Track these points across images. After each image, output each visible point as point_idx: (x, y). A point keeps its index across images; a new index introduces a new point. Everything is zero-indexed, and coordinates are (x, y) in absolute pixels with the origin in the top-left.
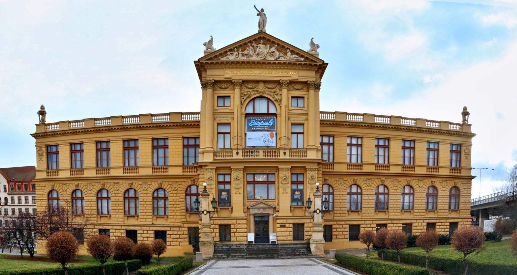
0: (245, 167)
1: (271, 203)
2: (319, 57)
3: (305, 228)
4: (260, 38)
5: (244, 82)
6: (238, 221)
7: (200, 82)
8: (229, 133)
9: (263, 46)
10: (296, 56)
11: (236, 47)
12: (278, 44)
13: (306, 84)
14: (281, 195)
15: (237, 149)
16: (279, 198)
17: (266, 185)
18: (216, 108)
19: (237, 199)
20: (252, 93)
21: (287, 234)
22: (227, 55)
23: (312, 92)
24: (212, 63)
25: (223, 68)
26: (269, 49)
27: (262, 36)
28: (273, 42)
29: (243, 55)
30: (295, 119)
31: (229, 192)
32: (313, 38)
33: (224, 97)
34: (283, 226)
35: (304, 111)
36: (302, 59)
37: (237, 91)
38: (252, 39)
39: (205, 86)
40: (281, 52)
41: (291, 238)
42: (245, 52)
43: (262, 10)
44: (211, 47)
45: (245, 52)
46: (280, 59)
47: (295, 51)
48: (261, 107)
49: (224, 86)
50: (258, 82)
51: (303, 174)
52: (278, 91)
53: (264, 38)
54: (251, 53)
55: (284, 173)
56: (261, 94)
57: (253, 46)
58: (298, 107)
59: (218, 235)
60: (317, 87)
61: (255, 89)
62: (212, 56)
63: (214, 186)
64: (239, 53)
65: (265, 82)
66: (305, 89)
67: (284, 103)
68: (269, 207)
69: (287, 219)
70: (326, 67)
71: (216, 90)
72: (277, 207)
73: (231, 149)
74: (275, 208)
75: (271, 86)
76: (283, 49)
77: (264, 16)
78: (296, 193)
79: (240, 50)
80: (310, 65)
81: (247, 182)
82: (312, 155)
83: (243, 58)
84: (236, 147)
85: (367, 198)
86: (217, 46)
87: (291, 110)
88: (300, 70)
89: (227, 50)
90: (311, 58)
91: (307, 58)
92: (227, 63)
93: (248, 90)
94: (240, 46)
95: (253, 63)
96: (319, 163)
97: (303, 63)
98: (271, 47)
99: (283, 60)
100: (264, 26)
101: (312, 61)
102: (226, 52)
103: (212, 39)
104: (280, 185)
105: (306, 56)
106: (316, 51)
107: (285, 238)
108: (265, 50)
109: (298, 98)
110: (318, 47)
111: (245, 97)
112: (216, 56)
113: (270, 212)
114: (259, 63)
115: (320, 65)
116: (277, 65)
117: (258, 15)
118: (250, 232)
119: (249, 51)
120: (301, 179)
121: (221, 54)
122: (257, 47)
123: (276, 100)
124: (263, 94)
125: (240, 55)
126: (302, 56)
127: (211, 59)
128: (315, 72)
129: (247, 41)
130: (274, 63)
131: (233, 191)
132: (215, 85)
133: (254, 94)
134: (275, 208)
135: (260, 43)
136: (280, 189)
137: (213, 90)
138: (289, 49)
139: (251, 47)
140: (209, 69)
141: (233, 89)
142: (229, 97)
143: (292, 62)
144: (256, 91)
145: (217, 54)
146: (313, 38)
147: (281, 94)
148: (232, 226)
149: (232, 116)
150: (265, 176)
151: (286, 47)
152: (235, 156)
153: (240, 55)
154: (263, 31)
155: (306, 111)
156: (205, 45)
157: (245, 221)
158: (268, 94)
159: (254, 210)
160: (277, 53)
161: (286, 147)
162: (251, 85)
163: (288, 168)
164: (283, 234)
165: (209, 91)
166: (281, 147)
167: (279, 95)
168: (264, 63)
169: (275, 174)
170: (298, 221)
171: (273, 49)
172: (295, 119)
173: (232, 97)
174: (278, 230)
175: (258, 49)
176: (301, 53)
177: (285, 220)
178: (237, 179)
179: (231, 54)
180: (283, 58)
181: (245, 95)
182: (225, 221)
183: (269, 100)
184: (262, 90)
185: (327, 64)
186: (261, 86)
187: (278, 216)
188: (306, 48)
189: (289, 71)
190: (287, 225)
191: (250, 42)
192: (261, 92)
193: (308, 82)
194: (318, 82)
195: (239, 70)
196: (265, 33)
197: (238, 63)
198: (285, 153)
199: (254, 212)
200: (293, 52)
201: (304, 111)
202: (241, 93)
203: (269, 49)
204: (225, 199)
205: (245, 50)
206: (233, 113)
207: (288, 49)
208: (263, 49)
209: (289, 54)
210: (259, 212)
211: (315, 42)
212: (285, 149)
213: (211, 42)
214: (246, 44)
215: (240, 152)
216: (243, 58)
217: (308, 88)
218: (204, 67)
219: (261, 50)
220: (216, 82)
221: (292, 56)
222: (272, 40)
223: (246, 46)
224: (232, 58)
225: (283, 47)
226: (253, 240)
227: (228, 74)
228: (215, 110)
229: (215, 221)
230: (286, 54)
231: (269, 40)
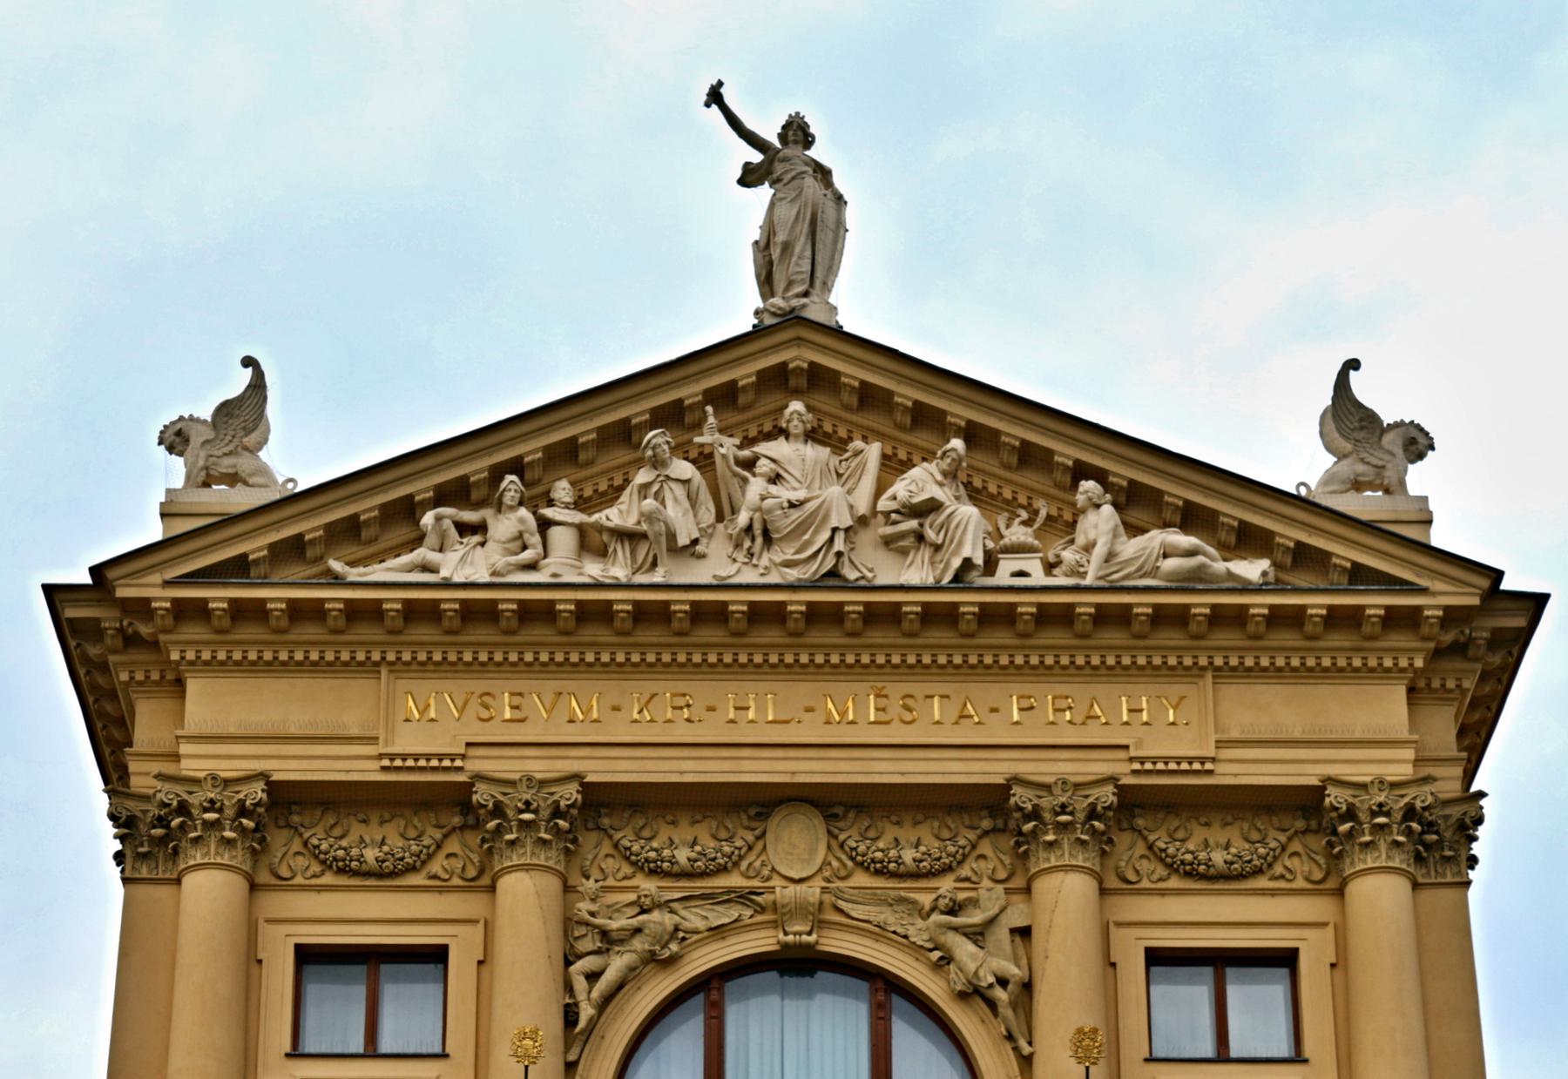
2: (1440, 537)
4: (778, 380)
5: (602, 804)
7: (103, 802)
9: (816, 453)
11: (516, 466)
12: (973, 435)
20: (694, 918)
22: (418, 540)
23: (1381, 893)
25: (370, 668)
26: (878, 493)
27: (798, 357)
29: (591, 543)
32: (1353, 364)
33: (371, 961)
36: (1252, 569)
37: (525, 895)
38: (690, 392)
39: (151, 839)
40: (1011, 506)
42: (616, 516)
44: (243, 463)
45: (616, 516)
46: (1003, 574)
47: (1158, 484)
49: (373, 841)
50: (760, 804)
52: (991, 898)
56: (798, 932)
57: (704, 460)
60: (1440, 839)
61: (734, 880)
62: (255, 547)
64: (544, 525)
66: (1302, 868)
67: (1064, 1006)
70: (1523, 638)
71: (283, 884)
75: (911, 843)
76: (1030, 478)
79: (563, 490)
83: (593, 569)
88: (1224, 673)
89: (421, 487)
90: (1344, 554)
91: (1304, 556)
93: (649, 885)
97: (1260, 603)
98: (893, 466)
99: (1038, 577)
100: (820, 274)
101: (1359, 576)
102: (408, 510)
103: (258, 386)
105: (1288, 534)
106: (1395, 488)
108: (835, 490)
109: (1221, 963)
110: (1417, 443)
111: (617, 965)
112: (295, 549)
114: (762, 615)
115: (1452, 616)
116: (971, 631)
117: (750, 177)
119: (664, 495)
121: (349, 531)
122: (749, 464)
123: (973, 994)
124: (820, 925)
125: (562, 539)
126: (1248, 540)
127: (238, 568)
128: (1398, 693)
129: (637, 410)
130: (938, 616)
132: (278, 839)
133: (718, 932)
135: (781, 432)
137: (254, 887)
138: (1100, 476)
139: (683, 469)
140: (212, 666)
141: (484, 883)
142: (436, 956)
143: (1142, 604)
144: (744, 897)
145: (310, 526)
146: (1353, 364)
147: (1024, 933)
151: (1067, 453)
153: (562, 539)
154: (814, 313)
156: (175, 439)
158: (880, 933)
160: (968, 512)
162: (683, 843)
165: (207, 889)
167: (1001, 934)
171: (921, 482)
173: (460, 964)
175: (756, 486)
176: (1232, 513)
179: (464, 529)
180: (1034, 566)
181: (609, 941)
183: (886, 990)
184: (812, 892)
185: (1537, 603)
186: (796, 855)
188: (1295, 459)
189: (1101, 690)
192: (800, 910)
193: (1336, 797)
194: (1449, 787)
195: (550, 686)
196: (838, 332)
197: (533, 614)
200: (1138, 507)
202: (569, 923)
203: (878, 493)
205: (611, 496)
207: (1081, 471)
208: (799, 472)
209: (1100, 523)
213: (244, 413)
214: (624, 435)
216: (593, 569)
217: (1335, 859)
219: (784, 493)
220: (288, 802)
221: (1131, 547)
222: (906, 394)
223: (622, 456)
224: (466, 565)
225: (1031, 452)
227: (427, 722)
230: (1064, 525)
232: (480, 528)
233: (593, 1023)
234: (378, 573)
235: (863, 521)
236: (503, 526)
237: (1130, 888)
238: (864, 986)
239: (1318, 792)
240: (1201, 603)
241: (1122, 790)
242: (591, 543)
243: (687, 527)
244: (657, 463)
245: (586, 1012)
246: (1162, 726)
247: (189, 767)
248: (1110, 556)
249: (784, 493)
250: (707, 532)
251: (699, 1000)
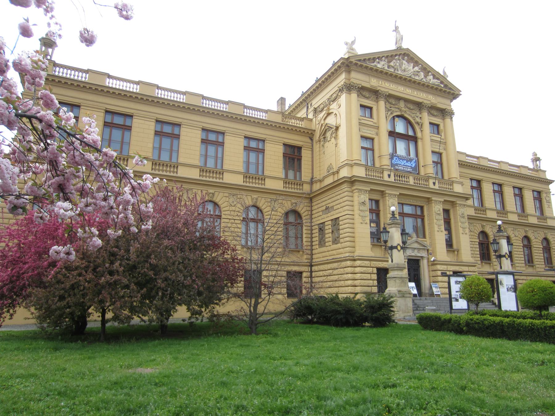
52: (418, 114)
55: (438, 206)
65: (406, 101)
80: (449, 93)
88: (438, 96)
113: (424, 254)
123: (418, 123)
140: (355, 71)
149: (376, 130)
206: (378, 128)
210: (413, 254)
227: (374, 82)
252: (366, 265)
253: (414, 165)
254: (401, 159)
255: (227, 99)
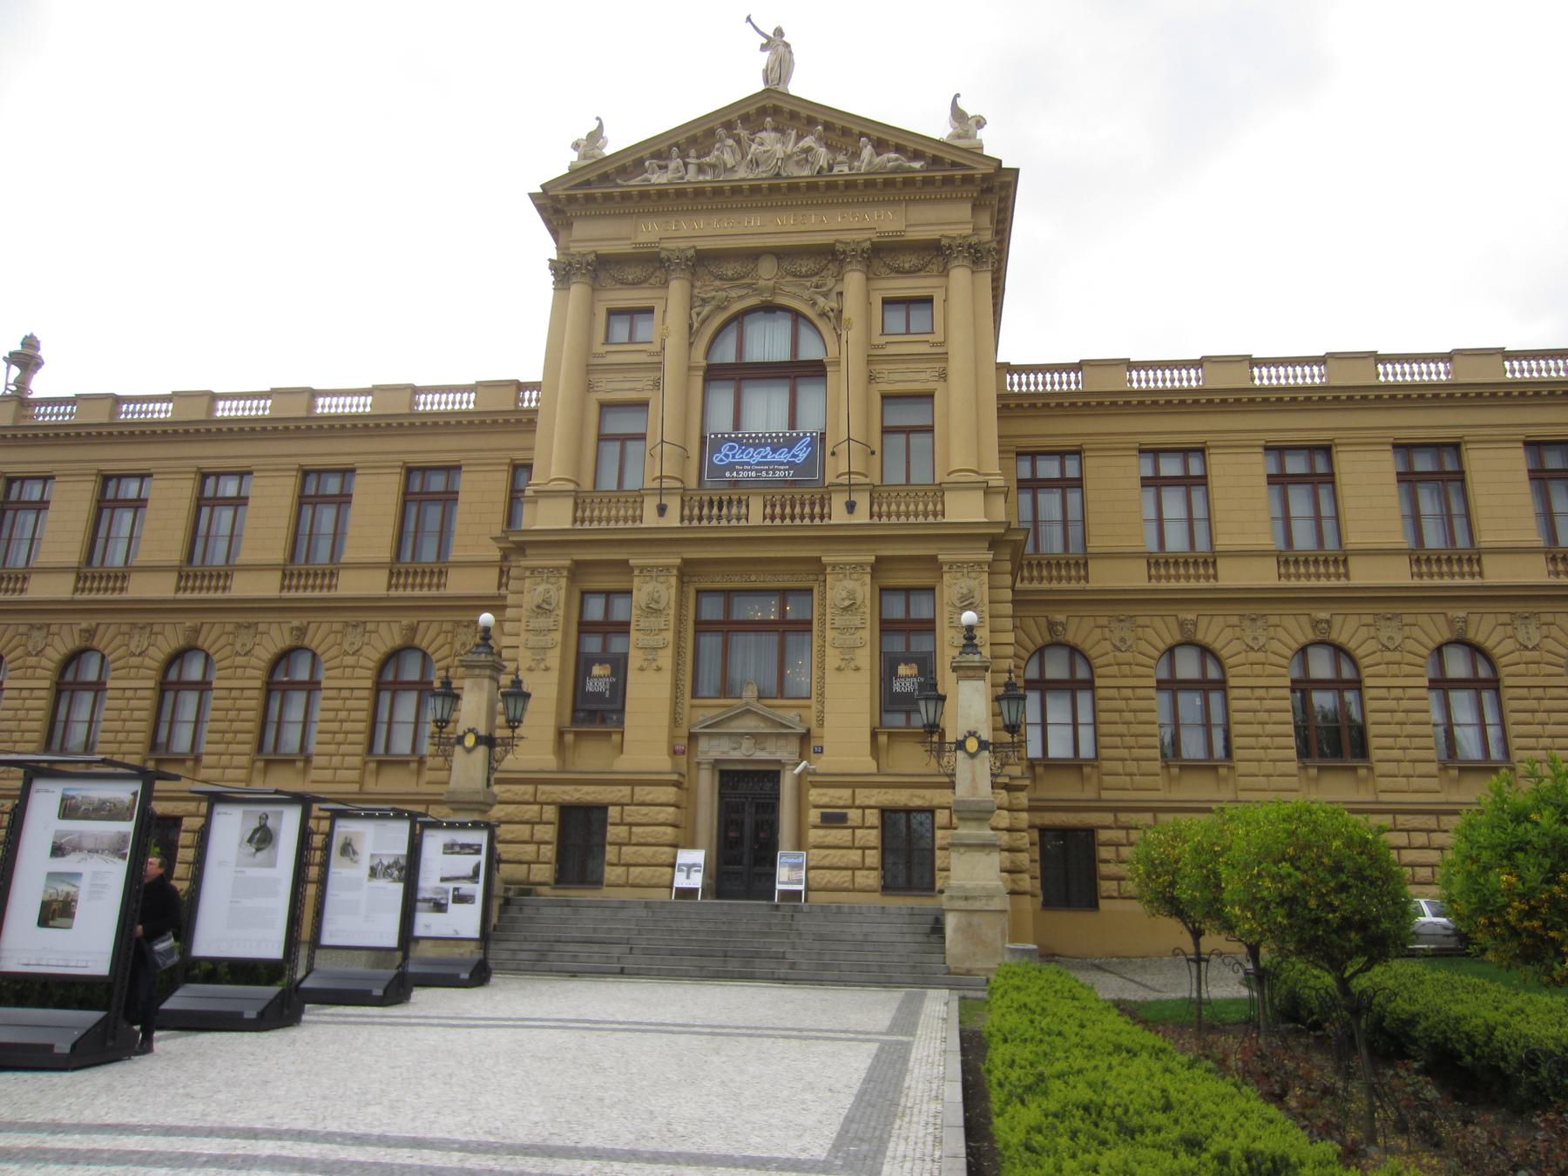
0: (686, 562)
1: (791, 715)
3: (939, 833)
4: (763, 112)
6: (642, 793)
8: (641, 437)
10: (893, 155)
11: (677, 145)
13: (936, 253)
14: (830, 676)
15: (661, 491)
16: (822, 694)
17: (773, 639)
18: (599, 348)
19: (649, 693)
20: (733, 294)
21: (854, 856)
24: (589, 199)
27: (769, 103)
28: (811, 122)
30: (897, 377)
31: (619, 666)
34: (833, 819)
35: (934, 345)
37: (677, 290)
38: (733, 116)
41: (872, 879)
43: (779, 32)
46: (835, 171)
48: (768, 342)
49: (631, 274)
50: (753, 255)
51: (932, 589)
52: (830, 282)
53: (776, 111)
54: (728, 159)
56: (767, 297)
57: (738, 141)
58: (908, 332)
59: (549, 852)
63: (558, 636)
64: (686, 165)
65: (782, 254)
68: (781, 732)
69: (853, 786)
72: (815, 731)
73: (639, 496)
74: (805, 738)
75: (805, 266)
77: (781, 49)
78: (903, 670)
79: (693, 152)
81: (697, 622)
82: (965, 509)
84: (656, 484)
85: (1255, 704)
86: (615, 143)
87: (882, 347)
92: (644, 195)
93: (717, 283)
94: (693, 141)
95: (736, 190)
96: (994, 542)
98: (800, 137)
99: (846, 170)
104: (830, 634)
107: (841, 877)
108: (778, 146)
113: (783, 752)
114: (755, 190)
116: (825, 191)
118: (692, 845)
120: (921, 609)
121: (623, 171)
123: (823, 315)
125: (692, 169)
127: (588, 183)
130: (812, 187)
131: (633, 663)
133: (741, 298)
134: (805, 738)
136: (829, 650)
139: (730, 142)
141: (665, 284)
144: (749, 286)
147: (841, 294)
148: (613, 813)
149: (653, 375)
150: (774, 602)
152: (650, 519)
153: (692, 169)
155: (941, 344)
157: (669, 794)
158: (794, 296)
159: (714, 742)
160: (823, 151)
161: (856, 479)
162: (730, 269)
163: (861, 565)
164: (835, 857)
165: (577, 290)
166: (839, 481)
168: (773, 189)
169: (810, 590)
170: (900, 798)
171: (808, 141)
172: (897, 377)
174: (814, 835)
175: (754, 146)
177: (847, 793)
178: (652, 611)
179: (661, 167)
180: (846, 170)
181: (704, 301)
182: (585, 789)
183: (797, 316)
186: (767, 271)
187: (815, 774)
188: (938, 128)
190: (854, 815)
191: (729, 126)
197: (681, 194)
198: (851, 506)
199: (716, 754)
201: (934, 345)
202: (692, 297)
204: (602, 694)
205: (708, 154)
207: (862, 135)
209: (867, 152)
210: (736, 755)
211: (969, 107)
212: (850, 487)
215: (674, 504)
218: (563, 212)
219: (762, 149)
224: (658, 179)
226: (696, 881)
227: (650, 232)
228: (596, 355)
229: (542, 788)
230: (856, 155)
231: (794, 116)
232: (666, 167)
233: (698, 330)
234: (632, 182)
235: (789, 157)
236: (672, 165)
237: (878, 277)
238: (788, 315)
239: (939, 241)
240: (899, 177)
241: (873, 244)
242: (701, 169)
243: (730, 162)
244: (721, 140)
245: (696, 325)
246: (886, 221)
247: (573, 250)
248: (870, 163)
249: (762, 149)
250: (738, 164)
251: (735, 324)
252: (518, 798)
253: (802, 456)
254: (748, 445)
255: (369, 385)
